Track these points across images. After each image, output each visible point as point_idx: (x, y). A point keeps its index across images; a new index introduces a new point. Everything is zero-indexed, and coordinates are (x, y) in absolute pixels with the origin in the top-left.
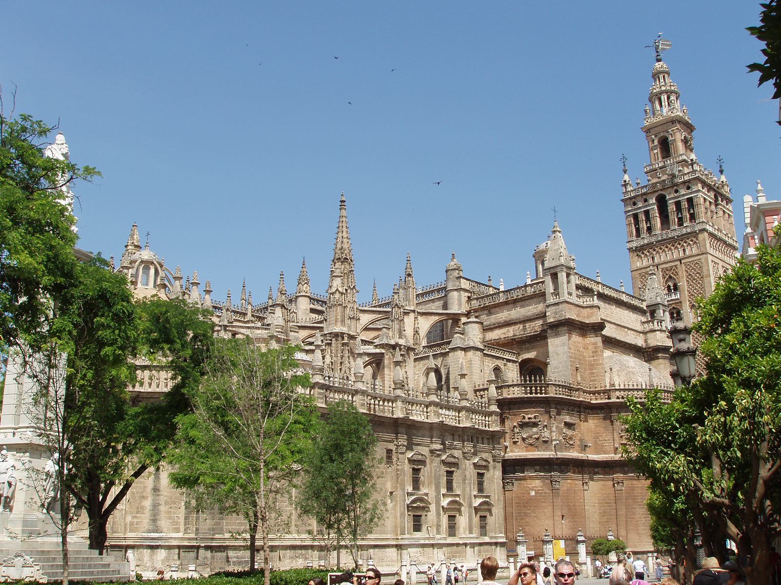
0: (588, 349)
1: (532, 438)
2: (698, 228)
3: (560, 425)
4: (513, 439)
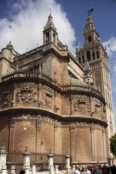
0: (61, 68)
1: (27, 99)
2: (99, 60)
3: (44, 95)
4: (17, 99)
